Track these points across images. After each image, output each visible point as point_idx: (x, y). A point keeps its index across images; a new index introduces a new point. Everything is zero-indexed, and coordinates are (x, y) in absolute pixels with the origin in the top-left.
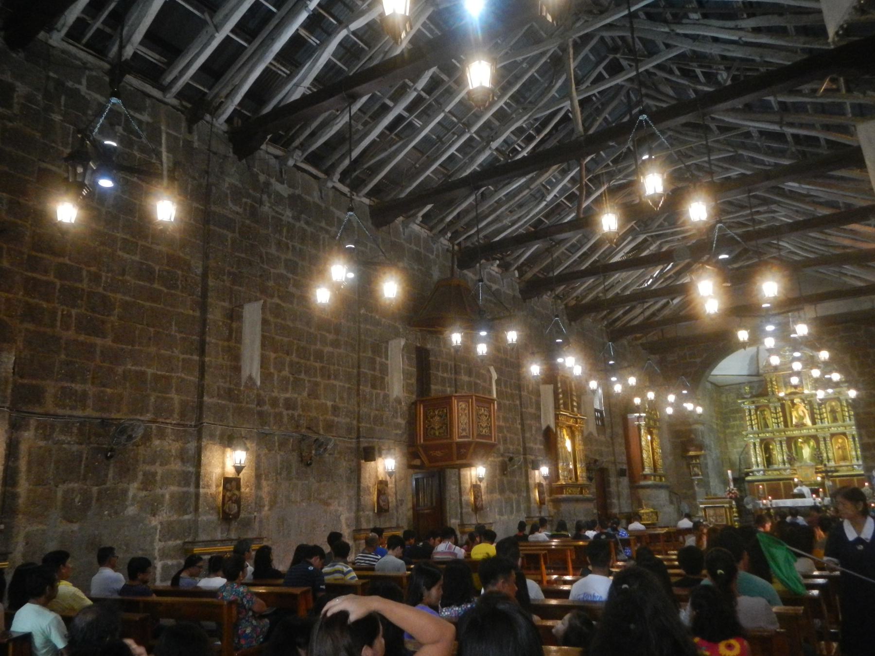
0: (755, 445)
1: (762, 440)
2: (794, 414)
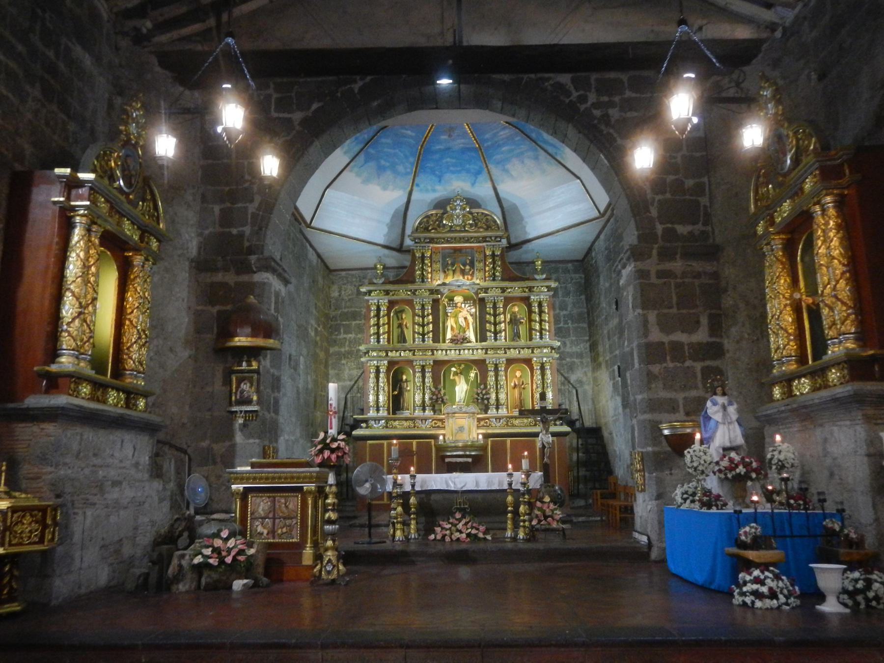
0: (378, 372)
1: (391, 364)
2: (450, 322)
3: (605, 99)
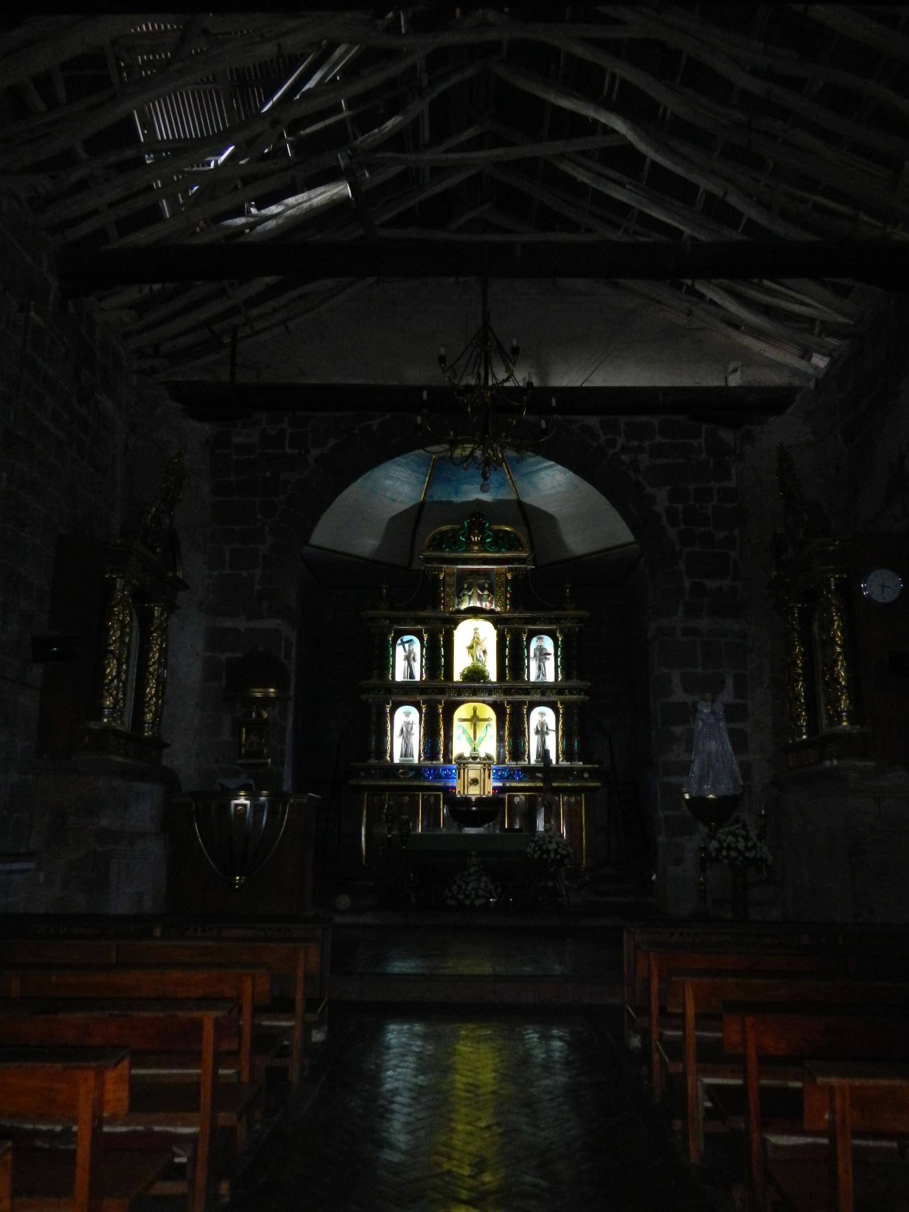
3: (636, 443)
